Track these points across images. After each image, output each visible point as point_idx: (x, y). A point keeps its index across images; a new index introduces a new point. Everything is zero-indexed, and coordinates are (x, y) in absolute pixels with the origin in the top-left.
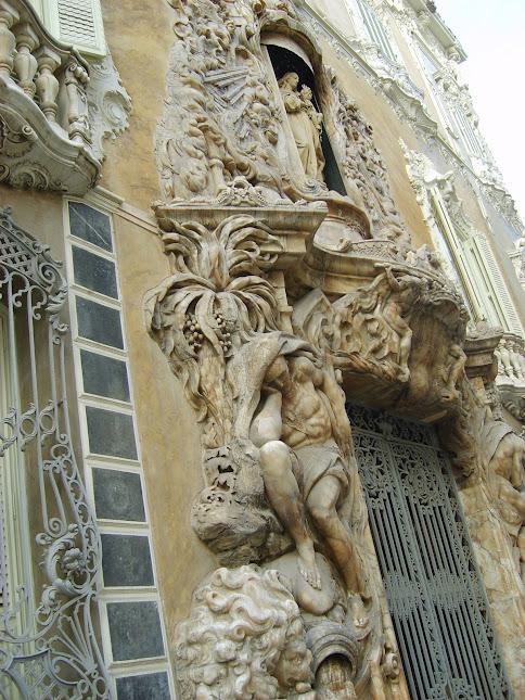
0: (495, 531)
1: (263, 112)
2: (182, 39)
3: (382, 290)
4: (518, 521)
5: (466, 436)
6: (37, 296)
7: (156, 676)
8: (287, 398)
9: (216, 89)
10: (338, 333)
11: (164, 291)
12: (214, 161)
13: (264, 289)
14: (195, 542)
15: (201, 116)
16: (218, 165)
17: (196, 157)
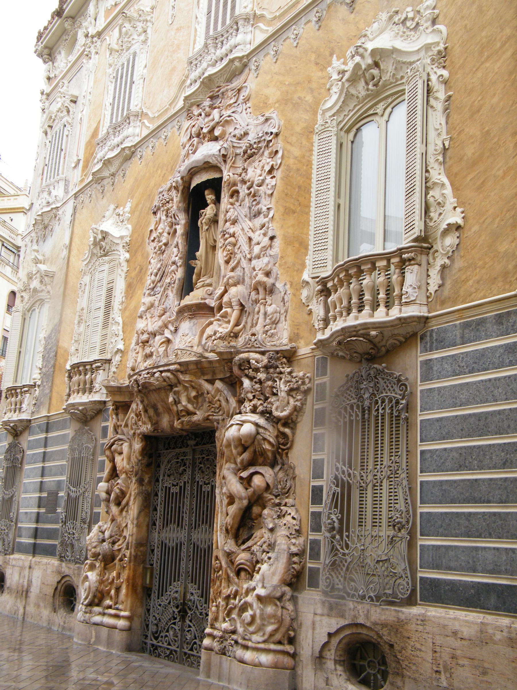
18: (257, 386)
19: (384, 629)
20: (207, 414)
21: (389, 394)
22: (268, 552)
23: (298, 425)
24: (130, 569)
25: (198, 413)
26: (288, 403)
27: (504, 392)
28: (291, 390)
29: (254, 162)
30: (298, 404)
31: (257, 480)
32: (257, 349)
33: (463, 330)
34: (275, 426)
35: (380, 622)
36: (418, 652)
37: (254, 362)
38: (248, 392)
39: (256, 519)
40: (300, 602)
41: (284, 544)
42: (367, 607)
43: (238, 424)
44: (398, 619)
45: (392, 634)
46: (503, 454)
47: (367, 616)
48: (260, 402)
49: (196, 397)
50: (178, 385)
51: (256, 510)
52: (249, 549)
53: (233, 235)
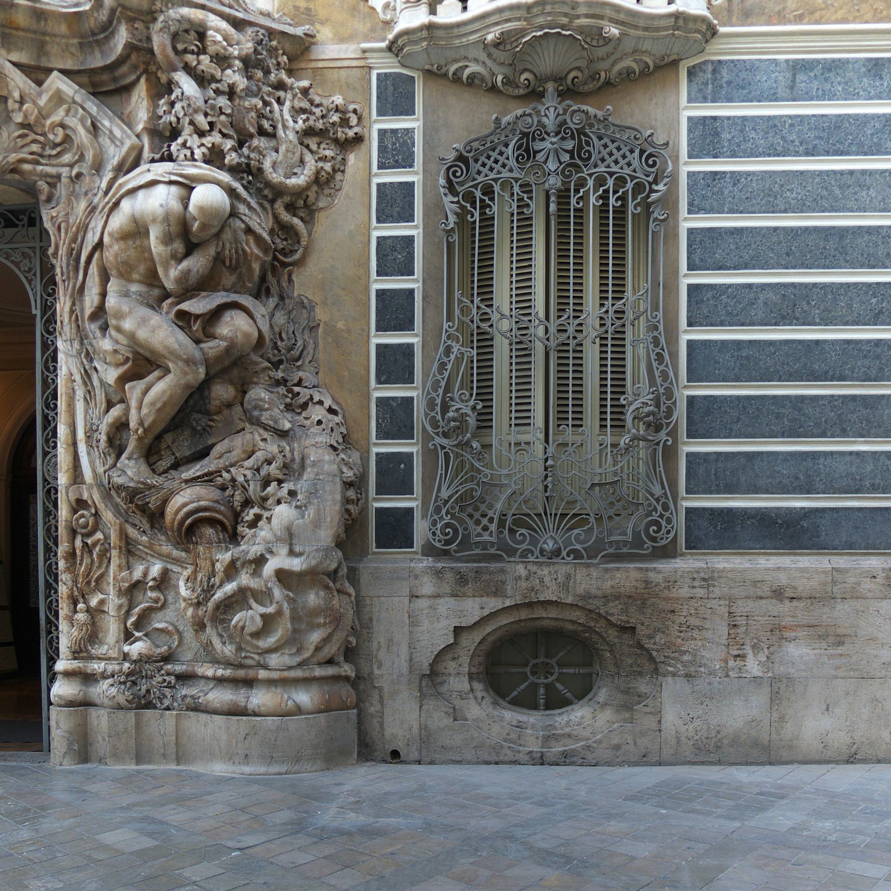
18: (223, 101)
19: (611, 604)
20: (13, 157)
21: (615, 169)
22: (280, 482)
23: (321, 217)
26: (302, 162)
27: (880, 198)
28: (309, 132)
31: (235, 326)
32: (227, 10)
33: (794, 76)
34: (267, 206)
35: (599, 593)
36: (695, 633)
37: (219, 38)
38: (196, 111)
39: (219, 412)
40: (364, 578)
41: (330, 462)
42: (568, 569)
43: (171, 183)
44: (647, 582)
45: (632, 609)
46: (874, 300)
47: (565, 586)
48: (229, 144)
51: (222, 392)
52: (208, 478)
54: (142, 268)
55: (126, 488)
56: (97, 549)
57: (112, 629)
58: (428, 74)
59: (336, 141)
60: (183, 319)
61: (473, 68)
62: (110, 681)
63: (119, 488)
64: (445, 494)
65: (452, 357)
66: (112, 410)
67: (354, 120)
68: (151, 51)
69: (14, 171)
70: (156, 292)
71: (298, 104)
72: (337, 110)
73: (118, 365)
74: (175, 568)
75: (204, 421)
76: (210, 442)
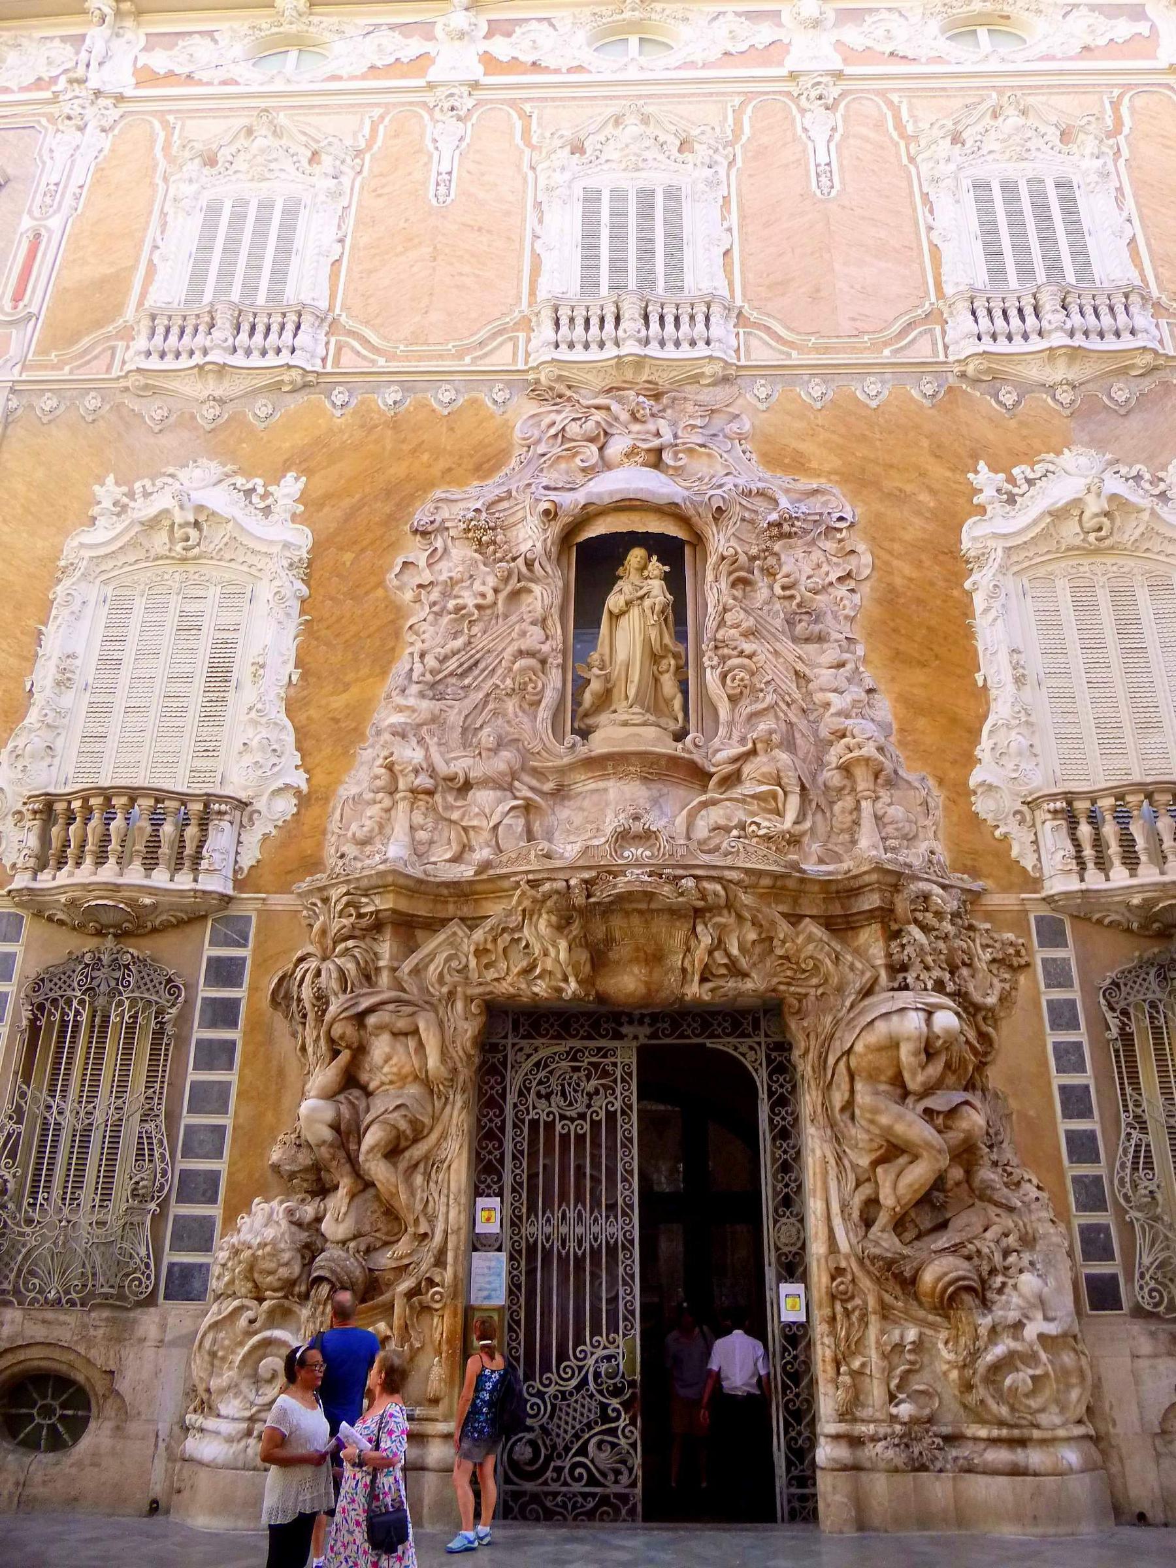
0: (810, 1160)
1: (523, 671)
2: (412, 644)
3: (527, 903)
4: (875, 1145)
5: (793, 1026)
6: (159, 1013)
7: (201, 1265)
8: (360, 1051)
9: (453, 680)
10: (473, 963)
11: (291, 966)
12: (398, 796)
13: (356, 952)
14: (269, 1173)
15: (386, 753)
16: (404, 798)
17: (375, 802)
18: (941, 945)
20: (775, 980)
24: (455, 1315)
25: (754, 975)
28: (994, 961)
29: (791, 547)
30: (1007, 986)
49: (754, 942)
50: (725, 912)
53: (750, 657)
54: (890, 1073)
55: (883, 1259)
56: (857, 1313)
57: (876, 1392)
58: (1074, 917)
59: (1011, 966)
60: (929, 1113)
61: (1114, 917)
62: (883, 1443)
63: (874, 1259)
64: (1146, 1261)
65: (1133, 1142)
66: (861, 1189)
67: (1023, 952)
68: (892, 911)
69: (774, 990)
70: (899, 1091)
71: (985, 942)
72: (1011, 944)
73: (871, 1151)
74: (929, 1332)
75: (941, 1196)
76: (948, 1215)
